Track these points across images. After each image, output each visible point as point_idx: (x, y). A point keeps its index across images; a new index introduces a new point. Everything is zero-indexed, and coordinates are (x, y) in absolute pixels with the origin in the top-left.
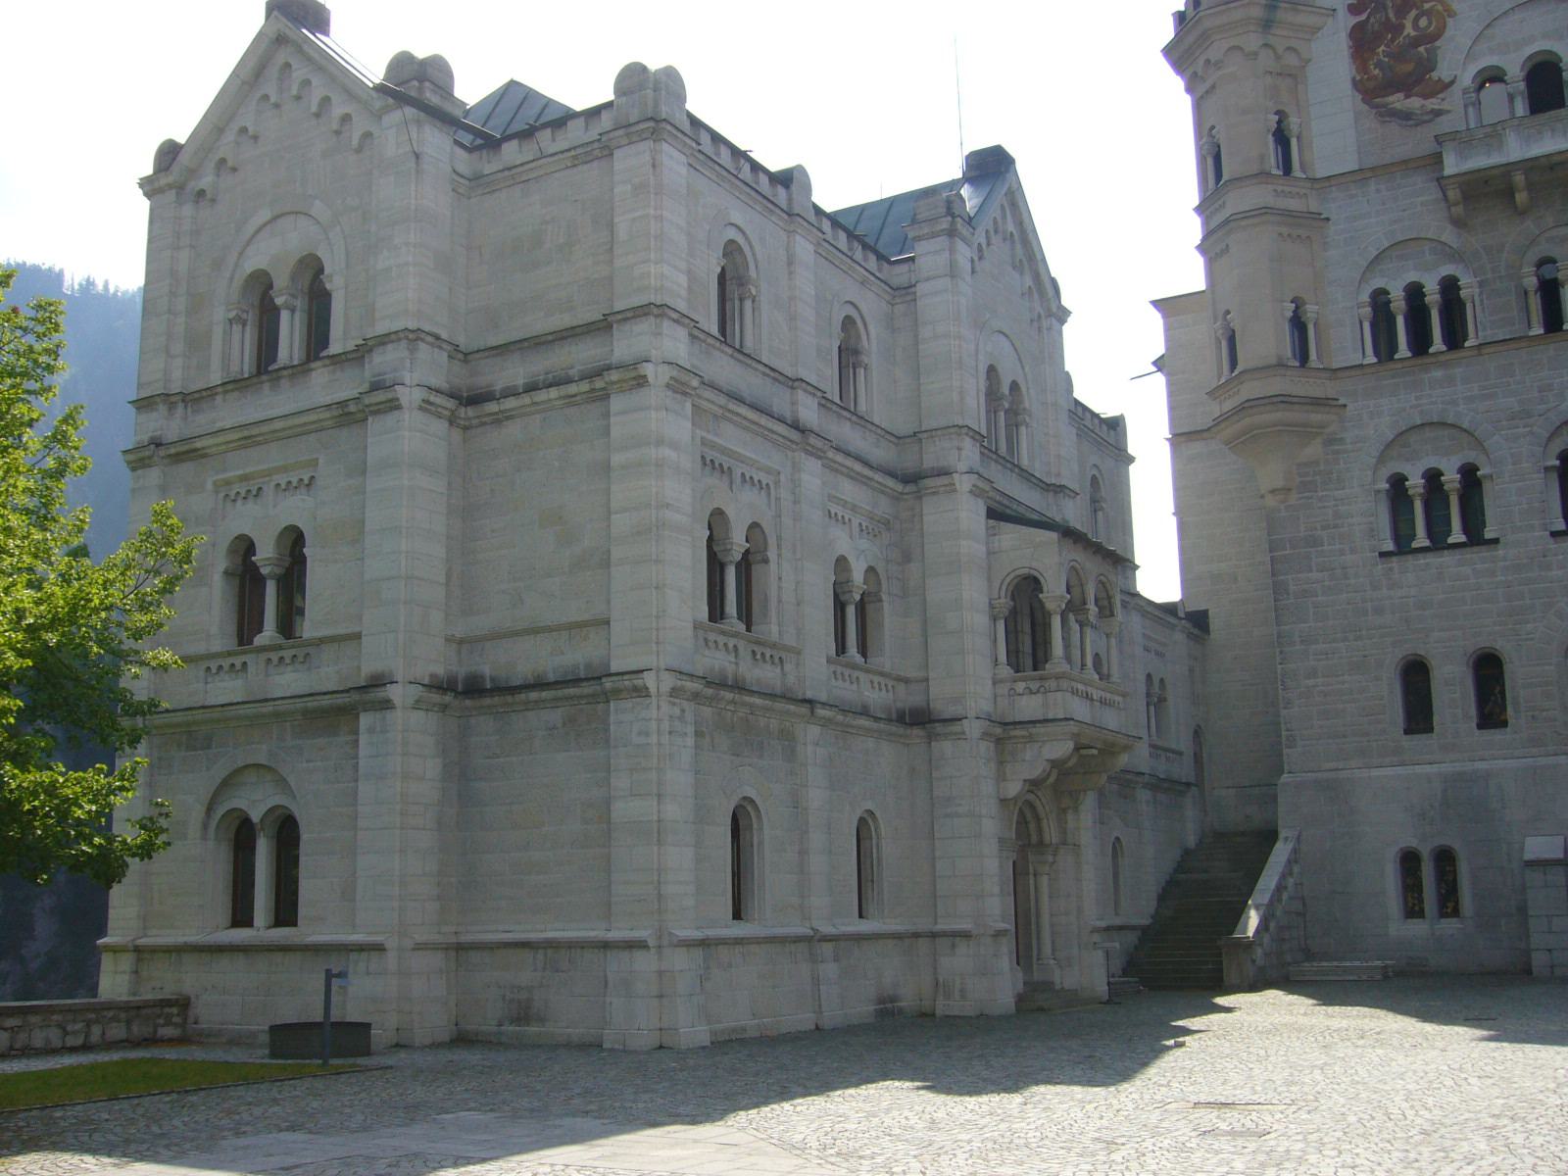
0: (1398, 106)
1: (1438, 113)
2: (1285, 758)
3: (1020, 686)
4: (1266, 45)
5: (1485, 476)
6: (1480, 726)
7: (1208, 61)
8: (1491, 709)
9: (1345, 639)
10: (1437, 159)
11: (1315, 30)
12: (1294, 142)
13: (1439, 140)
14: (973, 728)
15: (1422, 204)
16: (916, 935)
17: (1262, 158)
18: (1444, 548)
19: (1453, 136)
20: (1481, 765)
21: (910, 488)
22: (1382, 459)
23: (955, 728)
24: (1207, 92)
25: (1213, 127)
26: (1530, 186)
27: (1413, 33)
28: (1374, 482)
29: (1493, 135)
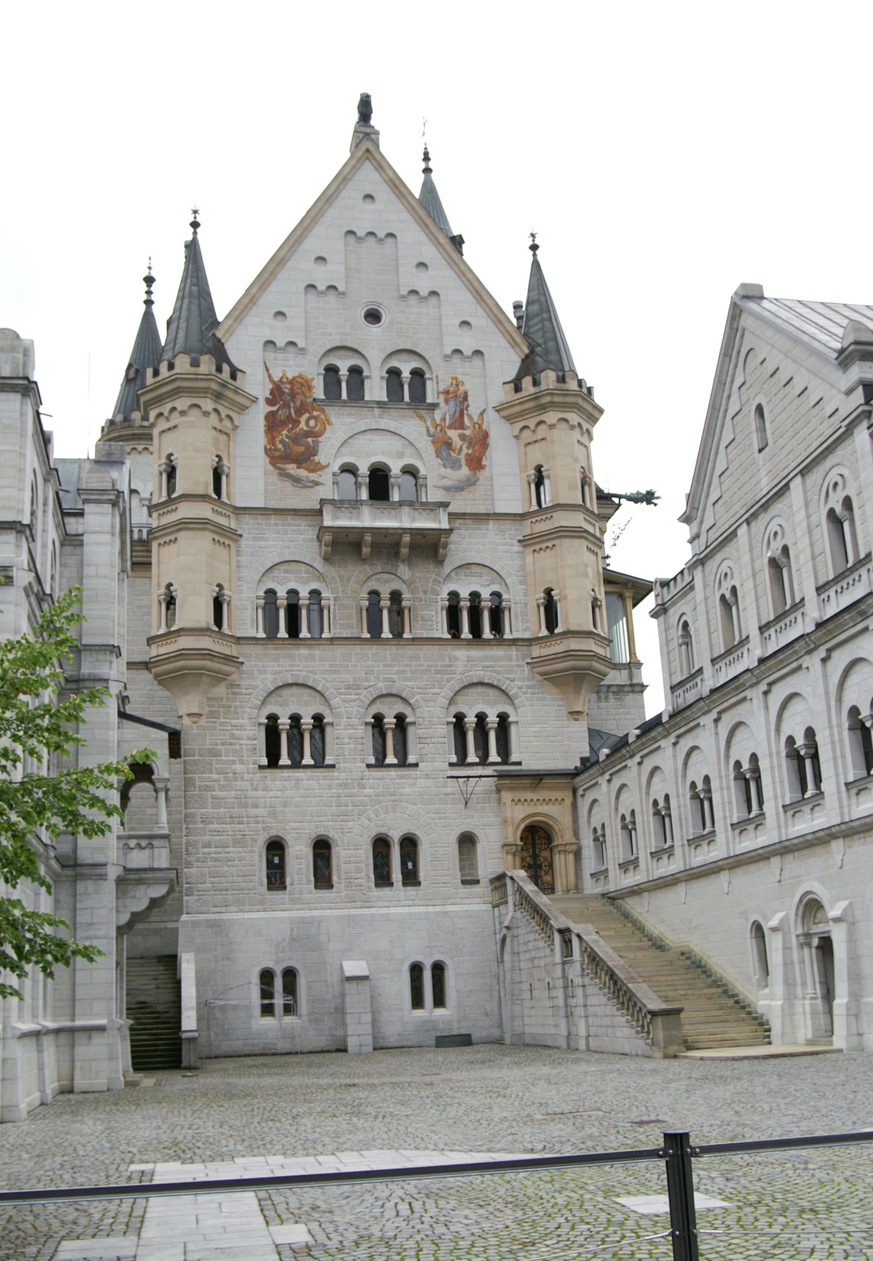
0: (292, 472)
1: (317, 484)
2: (185, 903)
3: (132, 843)
4: (216, 410)
5: (329, 723)
6: (316, 887)
7: (174, 409)
8: (323, 877)
9: (233, 823)
10: (320, 512)
11: (243, 408)
12: (224, 478)
13: (323, 502)
14: (113, 872)
15: (303, 539)
16: (58, 1031)
17: (207, 484)
18: (323, 767)
19: (332, 502)
20: (315, 913)
21: (73, 686)
22: (263, 703)
23: (99, 871)
24: (169, 429)
25: (171, 455)
26: (374, 546)
27: (305, 428)
28: (258, 717)
29: (355, 504)
